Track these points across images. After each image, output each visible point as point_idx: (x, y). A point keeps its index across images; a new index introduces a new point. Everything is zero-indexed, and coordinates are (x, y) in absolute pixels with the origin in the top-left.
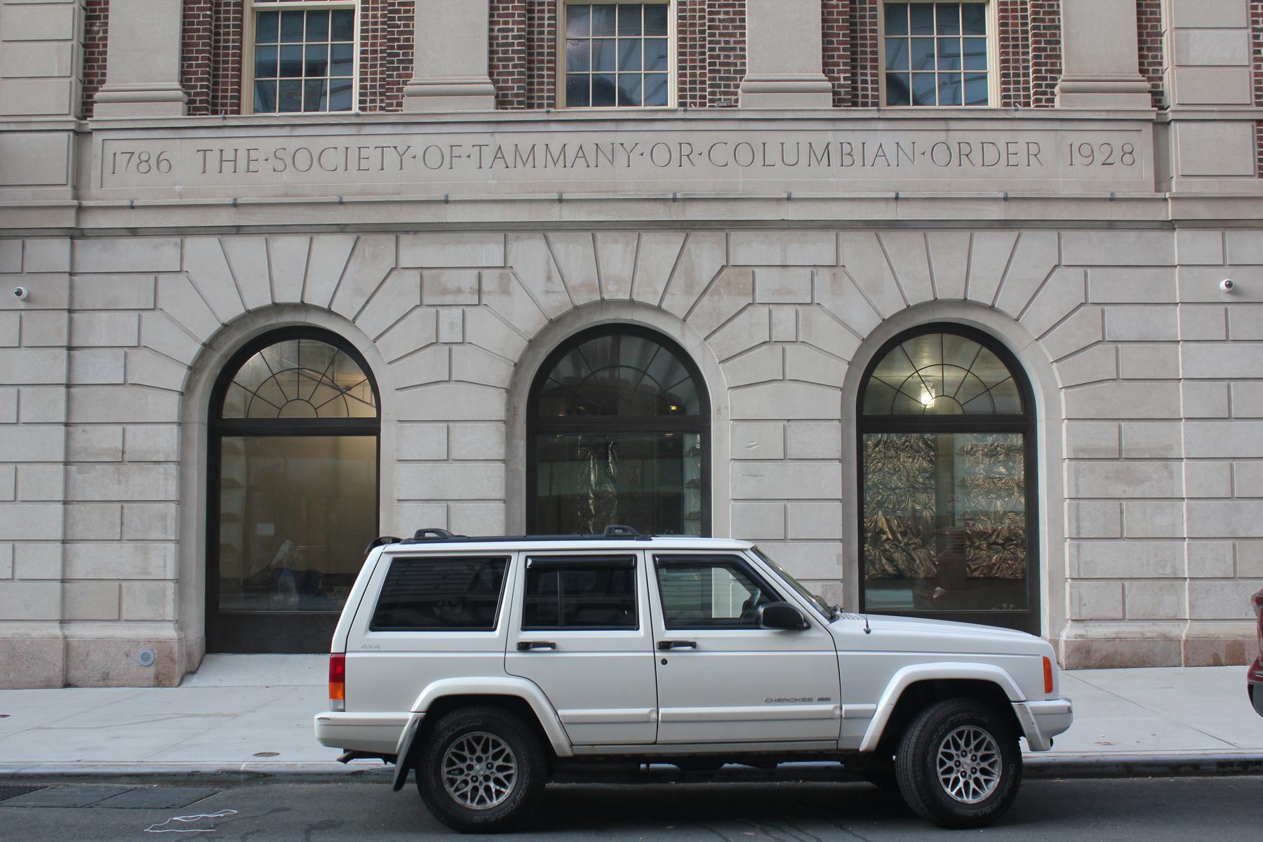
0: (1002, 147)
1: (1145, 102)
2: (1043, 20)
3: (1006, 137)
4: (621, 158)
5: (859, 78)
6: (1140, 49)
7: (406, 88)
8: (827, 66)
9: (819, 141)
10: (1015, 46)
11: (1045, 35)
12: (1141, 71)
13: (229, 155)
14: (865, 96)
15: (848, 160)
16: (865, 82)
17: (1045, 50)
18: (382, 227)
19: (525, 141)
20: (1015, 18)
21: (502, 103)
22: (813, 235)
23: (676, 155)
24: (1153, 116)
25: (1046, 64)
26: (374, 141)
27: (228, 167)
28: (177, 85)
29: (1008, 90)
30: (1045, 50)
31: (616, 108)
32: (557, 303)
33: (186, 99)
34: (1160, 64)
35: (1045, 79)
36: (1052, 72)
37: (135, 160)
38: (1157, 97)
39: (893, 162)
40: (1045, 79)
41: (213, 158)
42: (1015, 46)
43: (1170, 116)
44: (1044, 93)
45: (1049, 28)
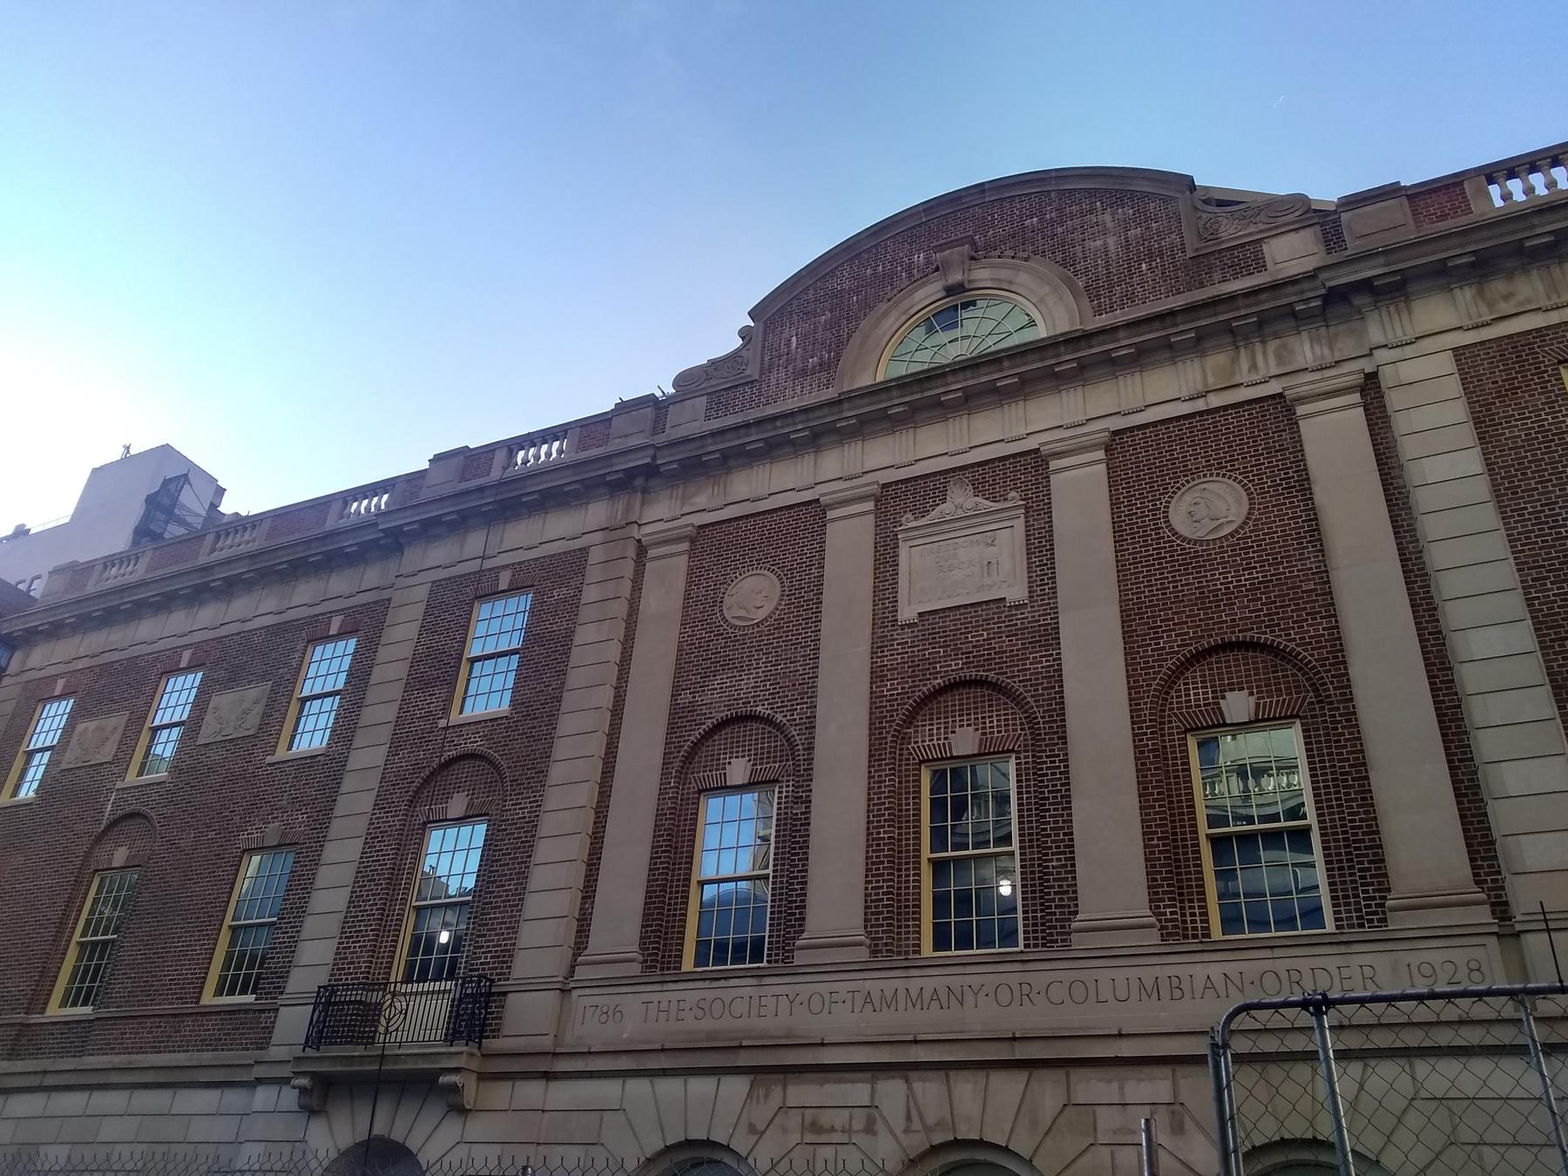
0: (1335, 972)
1: (1483, 915)
2: (1363, 841)
3: (1338, 961)
4: (969, 997)
5: (1188, 912)
6: (1472, 860)
7: (798, 943)
8: (1154, 899)
9: (1148, 975)
10: (1340, 868)
11: (1367, 855)
12: (1477, 883)
13: (664, 1006)
14: (1195, 929)
15: (1177, 993)
16: (1193, 914)
17: (1369, 869)
18: (773, 1066)
19: (889, 987)
20: (1337, 840)
21: (875, 952)
23: (1017, 993)
24: (1495, 929)
25: (1372, 884)
26: (776, 987)
27: (663, 1016)
28: (635, 948)
29: (1339, 912)
30: (1369, 869)
31: (954, 953)
33: (641, 958)
34: (1499, 873)
35: (1374, 898)
36: (1379, 891)
37: (598, 1012)
38: (1501, 908)
39: (1223, 994)
40: (1374, 898)
42: (1340, 868)
43: (1518, 927)
44: (1376, 913)
45: (1371, 848)
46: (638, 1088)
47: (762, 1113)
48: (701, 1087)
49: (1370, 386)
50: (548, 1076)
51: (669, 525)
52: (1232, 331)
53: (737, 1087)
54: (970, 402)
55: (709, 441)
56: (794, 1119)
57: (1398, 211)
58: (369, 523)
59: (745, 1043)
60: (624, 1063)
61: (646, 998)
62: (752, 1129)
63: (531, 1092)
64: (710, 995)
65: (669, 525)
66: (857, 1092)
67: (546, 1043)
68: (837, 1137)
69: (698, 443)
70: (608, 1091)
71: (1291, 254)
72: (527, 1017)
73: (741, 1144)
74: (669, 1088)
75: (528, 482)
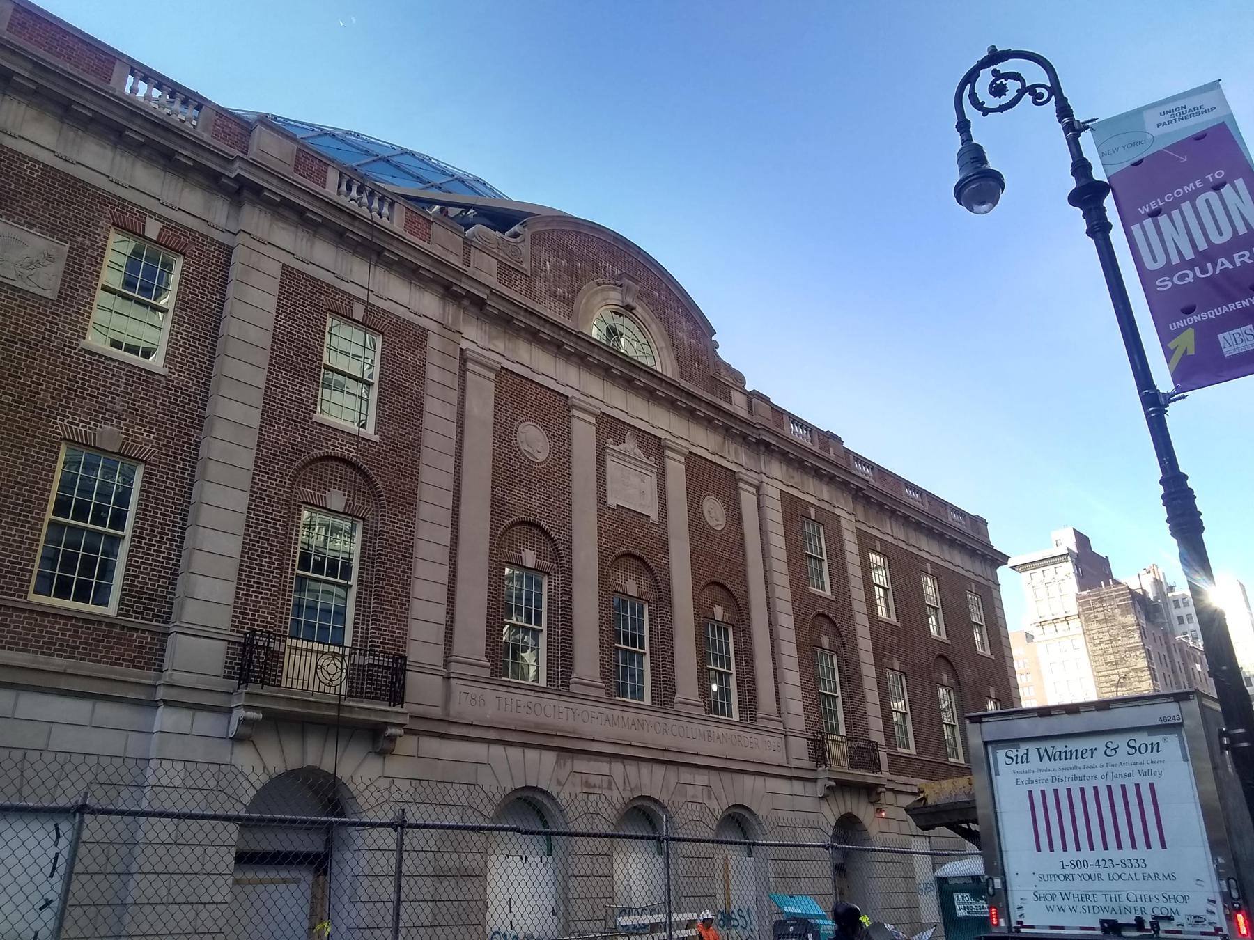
13: (509, 702)
22: (702, 771)
32: (628, 795)
41: (502, 701)
46: (497, 750)
47: (563, 774)
48: (532, 754)
49: (758, 489)
50: (442, 736)
51: (479, 350)
52: (727, 431)
53: (550, 757)
54: (650, 394)
55: (522, 312)
56: (578, 778)
57: (769, 414)
58: (133, 110)
59: (69, 671)
60: (492, 735)
61: (500, 694)
62: (559, 783)
63: (432, 746)
64: (534, 700)
65: (479, 350)
66: (603, 767)
67: (437, 712)
68: (596, 791)
69: (515, 309)
70: (479, 751)
71: (738, 405)
72: (423, 689)
73: (553, 790)
74: (515, 753)
75: (395, 243)
